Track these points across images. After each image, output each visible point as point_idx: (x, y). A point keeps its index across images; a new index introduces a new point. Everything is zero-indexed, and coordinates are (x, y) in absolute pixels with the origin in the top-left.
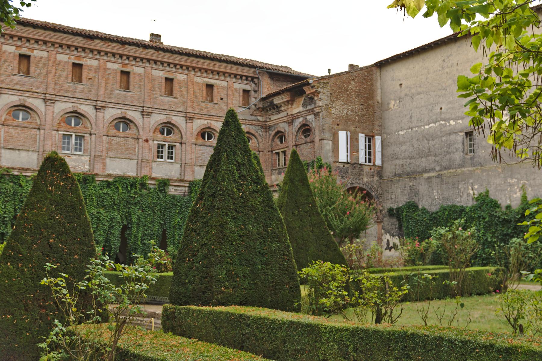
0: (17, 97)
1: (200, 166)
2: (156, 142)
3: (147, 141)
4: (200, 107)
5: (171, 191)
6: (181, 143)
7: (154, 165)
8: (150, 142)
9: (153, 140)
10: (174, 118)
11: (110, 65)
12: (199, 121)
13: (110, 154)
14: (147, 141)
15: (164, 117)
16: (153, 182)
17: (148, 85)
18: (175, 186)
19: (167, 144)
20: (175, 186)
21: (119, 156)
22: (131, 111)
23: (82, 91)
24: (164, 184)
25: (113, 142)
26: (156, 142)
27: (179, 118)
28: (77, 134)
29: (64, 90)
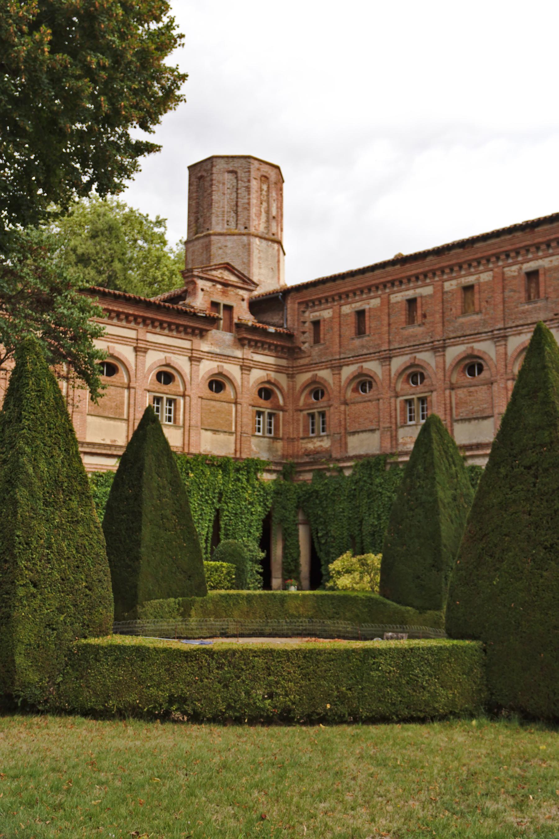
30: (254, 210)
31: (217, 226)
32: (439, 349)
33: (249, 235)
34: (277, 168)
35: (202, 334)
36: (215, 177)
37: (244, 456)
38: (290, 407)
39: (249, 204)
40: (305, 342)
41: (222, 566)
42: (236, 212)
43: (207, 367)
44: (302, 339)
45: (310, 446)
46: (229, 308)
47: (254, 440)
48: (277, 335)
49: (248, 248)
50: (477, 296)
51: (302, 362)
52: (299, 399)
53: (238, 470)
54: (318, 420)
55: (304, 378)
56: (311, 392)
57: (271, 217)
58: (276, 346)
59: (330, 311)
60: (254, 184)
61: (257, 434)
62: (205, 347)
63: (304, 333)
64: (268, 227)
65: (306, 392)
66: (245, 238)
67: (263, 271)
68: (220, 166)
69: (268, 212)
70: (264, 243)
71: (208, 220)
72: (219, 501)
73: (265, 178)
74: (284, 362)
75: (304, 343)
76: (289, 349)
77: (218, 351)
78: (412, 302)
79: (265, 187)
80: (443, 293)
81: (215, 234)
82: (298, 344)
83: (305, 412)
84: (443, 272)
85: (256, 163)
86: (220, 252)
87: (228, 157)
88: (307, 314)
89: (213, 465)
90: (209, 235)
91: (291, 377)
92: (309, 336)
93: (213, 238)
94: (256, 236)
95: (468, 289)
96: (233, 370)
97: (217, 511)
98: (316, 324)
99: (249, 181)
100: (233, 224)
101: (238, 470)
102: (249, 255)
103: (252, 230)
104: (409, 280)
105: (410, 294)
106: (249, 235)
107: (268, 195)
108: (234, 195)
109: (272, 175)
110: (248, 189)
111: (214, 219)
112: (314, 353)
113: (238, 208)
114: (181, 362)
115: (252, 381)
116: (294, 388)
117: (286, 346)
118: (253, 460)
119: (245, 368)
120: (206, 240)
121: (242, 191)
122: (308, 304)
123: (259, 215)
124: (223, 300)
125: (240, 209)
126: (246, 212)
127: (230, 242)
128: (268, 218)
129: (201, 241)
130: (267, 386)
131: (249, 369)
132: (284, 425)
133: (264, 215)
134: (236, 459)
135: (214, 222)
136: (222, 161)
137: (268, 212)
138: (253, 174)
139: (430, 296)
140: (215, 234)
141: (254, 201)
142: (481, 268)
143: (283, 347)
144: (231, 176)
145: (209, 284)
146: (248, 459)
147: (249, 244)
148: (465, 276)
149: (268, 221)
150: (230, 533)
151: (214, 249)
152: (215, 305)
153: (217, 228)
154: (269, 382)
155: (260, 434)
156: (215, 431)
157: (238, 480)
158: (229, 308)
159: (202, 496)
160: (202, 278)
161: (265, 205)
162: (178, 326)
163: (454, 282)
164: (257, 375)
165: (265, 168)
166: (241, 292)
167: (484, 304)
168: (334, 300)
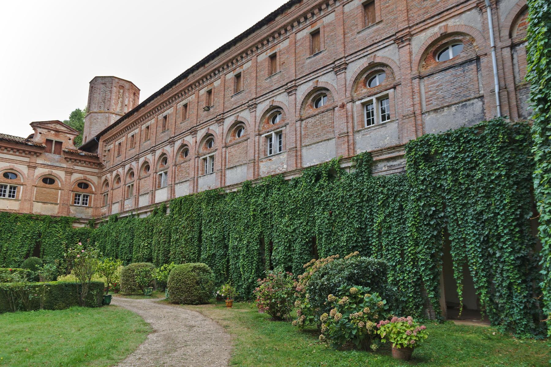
0: (233, 116)
1: (435, 110)
2: (358, 103)
3: (343, 106)
4: (422, 11)
5: (382, 170)
6: (394, 88)
7: (358, 137)
8: (349, 106)
9: (353, 101)
10: (379, 54)
11: (300, 36)
12: (423, 34)
13: (306, 142)
14: (343, 106)
15: (365, 59)
16: (350, 164)
17: (340, 31)
18: (388, 160)
19: (374, 98)
20: (388, 160)
21: (316, 140)
22: (323, 76)
23: (279, 81)
24: (367, 162)
25: (309, 125)
26: (358, 103)
27: (387, 49)
28: (276, 131)
29: (263, 90)
30: (113, 102)
35: (38, 155)
39: (110, 98)
42: (104, 102)
43: (40, 171)
44: (103, 159)
46: (59, 144)
51: (104, 170)
57: (124, 105)
60: (115, 89)
62: (40, 161)
66: (107, 114)
68: (100, 81)
69: (122, 103)
73: (122, 87)
74: (96, 171)
75: (104, 161)
77: (49, 163)
79: (121, 91)
81: (93, 113)
85: (117, 80)
86: (95, 121)
87: (102, 77)
91: (100, 177)
93: (92, 114)
94: (113, 114)
96: (61, 174)
99: (112, 88)
103: (112, 111)
110: (111, 92)
114: (23, 169)
115: (72, 180)
119: (69, 173)
123: (116, 104)
124: (55, 139)
125: (106, 101)
127: (100, 116)
131: (71, 173)
132: (94, 201)
136: (100, 79)
137: (122, 103)
138: (114, 84)
140: (93, 113)
141: (114, 97)
144: (103, 86)
145: (46, 131)
147: (109, 117)
152: (49, 141)
153: (95, 110)
156: (44, 203)
158: (59, 144)
160: (40, 128)
162: (18, 150)
164: (76, 176)
166: (68, 135)
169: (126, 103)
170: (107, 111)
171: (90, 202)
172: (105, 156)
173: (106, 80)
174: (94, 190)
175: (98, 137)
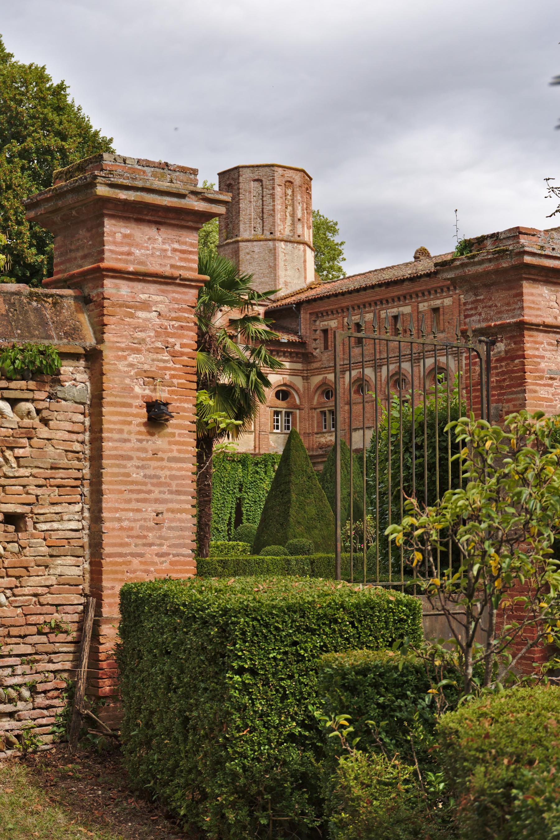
30: (278, 216)
31: (245, 233)
32: (415, 360)
33: (274, 240)
34: (304, 171)
36: (241, 185)
37: (262, 452)
38: (306, 405)
39: (274, 210)
40: (316, 347)
41: (238, 545)
44: (314, 345)
45: (323, 440)
47: (272, 437)
48: (290, 344)
49: (273, 252)
50: (441, 317)
51: (315, 365)
52: (313, 399)
53: (256, 464)
54: (329, 417)
55: (316, 380)
56: (322, 393)
57: (296, 219)
58: (291, 353)
59: (336, 321)
60: (279, 191)
61: (275, 431)
63: (315, 340)
64: (293, 230)
65: (319, 392)
66: (271, 243)
67: (289, 273)
68: (246, 175)
69: (293, 215)
70: (290, 245)
71: (236, 227)
72: (240, 490)
74: (299, 366)
75: (316, 349)
76: (303, 354)
78: (396, 318)
79: (289, 192)
80: (418, 312)
81: (243, 241)
82: (310, 350)
83: (318, 410)
84: (417, 296)
86: (248, 257)
87: (253, 167)
88: (318, 323)
89: (233, 461)
90: (238, 242)
91: (306, 379)
92: (320, 343)
93: (241, 244)
94: (281, 241)
95: (436, 310)
97: (239, 499)
98: (325, 331)
99: (273, 188)
100: (259, 230)
101: (256, 464)
102: (275, 259)
103: (278, 235)
104: (393, 301)
105: (394, 311)
106: (274, 240)
107: (293, 199)
108: (260, 201)
109: (297, 178)
110: (273, 196)
111: (242, 226)
112: (324, 358)
113: (264, 215)
116: (308, 389)
117: (300, 352)
118: (269, 455)
120: (236, 246)
121: (267, 198)
122: (318, 315)
123: (284, 220)
125: (265, 216)
126: (271, 219)
127: (257, 247)
128: (293, 221)
129: (231, 246)
130: (284, 388)
132: (300, 422)
133: (289, 218)
134: (255, 455)
135: (241, 229)
136: (248, 170)
137: (293, 215)
138: (277, 181)
139: (410, 315)
141: (278, 207)
142: (444, 294)
143: (297, 354)
144: (257, 184)
146: (265, 455)
147: (275, 249)
148: (433, 299)
149: (293, 224)
150: (251, 518)
151: (242, 255)
154: (285, 385)
155: (279, 431)
157: (257, 472)
159: (223, 488)
161: (290, 208)
163: (426, 304)
165: (289, 174)
167: (447, 324)
168: (338, 313)
169: (299, 215)
170: (270, 237)
171: (294, 424)
172: (315, 340)
173: (262, 172)
174: (298, 401)
175: (299, 304)
